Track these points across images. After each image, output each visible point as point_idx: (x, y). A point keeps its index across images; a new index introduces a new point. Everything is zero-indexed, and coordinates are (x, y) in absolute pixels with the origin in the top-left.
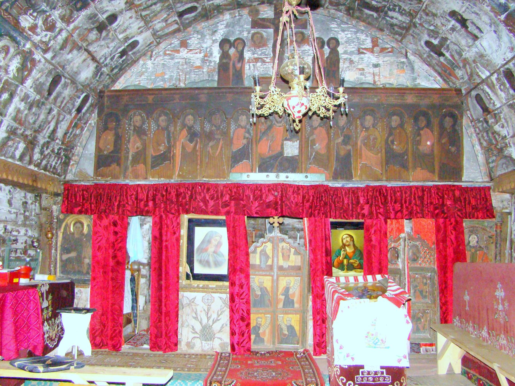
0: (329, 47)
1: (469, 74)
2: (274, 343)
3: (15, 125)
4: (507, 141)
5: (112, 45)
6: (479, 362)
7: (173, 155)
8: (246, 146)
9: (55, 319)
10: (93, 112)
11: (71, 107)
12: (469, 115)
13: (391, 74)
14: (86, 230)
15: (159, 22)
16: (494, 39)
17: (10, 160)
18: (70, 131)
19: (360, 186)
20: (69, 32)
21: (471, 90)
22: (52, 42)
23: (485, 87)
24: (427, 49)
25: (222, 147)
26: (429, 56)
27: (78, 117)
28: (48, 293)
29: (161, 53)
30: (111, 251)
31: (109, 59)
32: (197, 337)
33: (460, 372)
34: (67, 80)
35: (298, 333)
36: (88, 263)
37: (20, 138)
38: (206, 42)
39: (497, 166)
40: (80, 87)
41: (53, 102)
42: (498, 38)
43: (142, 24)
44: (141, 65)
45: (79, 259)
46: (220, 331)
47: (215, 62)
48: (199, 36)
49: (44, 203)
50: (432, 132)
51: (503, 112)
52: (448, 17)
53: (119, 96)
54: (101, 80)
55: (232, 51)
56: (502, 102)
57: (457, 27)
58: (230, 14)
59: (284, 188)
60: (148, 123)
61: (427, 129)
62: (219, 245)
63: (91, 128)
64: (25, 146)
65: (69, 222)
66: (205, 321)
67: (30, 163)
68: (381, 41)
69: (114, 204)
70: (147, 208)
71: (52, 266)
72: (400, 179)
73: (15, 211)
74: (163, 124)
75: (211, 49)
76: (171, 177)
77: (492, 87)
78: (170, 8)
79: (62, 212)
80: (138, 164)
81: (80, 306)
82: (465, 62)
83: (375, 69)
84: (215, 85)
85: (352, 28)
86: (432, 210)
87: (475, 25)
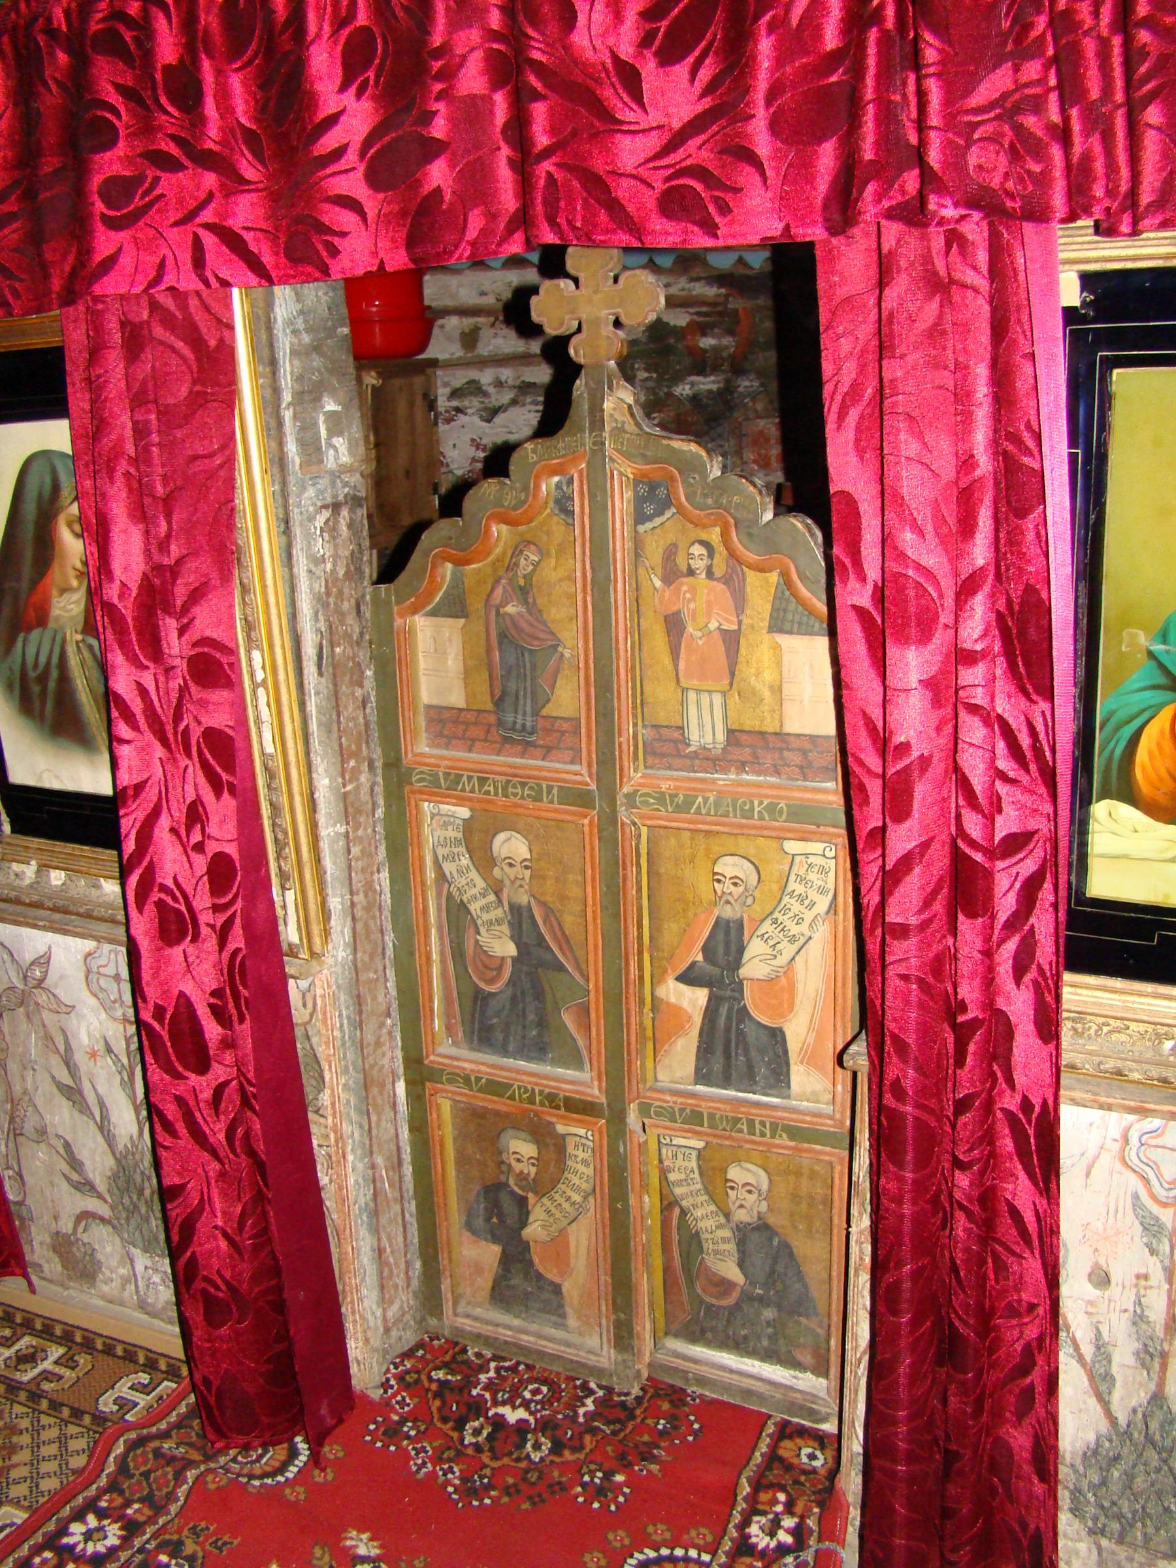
32: (102, 1219)
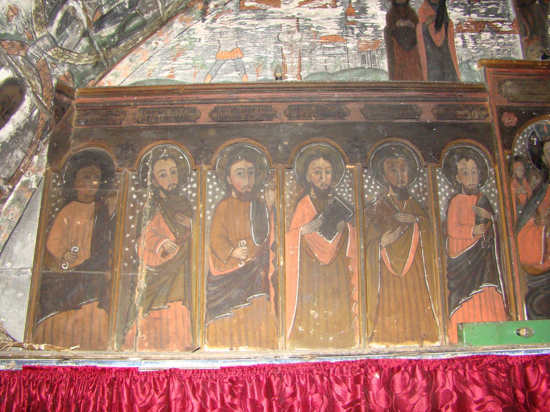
7: (276, 274)
8: (486, 244)
44: (176, 33)
47: (375, 27)
53: (115, 106)
63: (27, 196)
84: (385, 78)
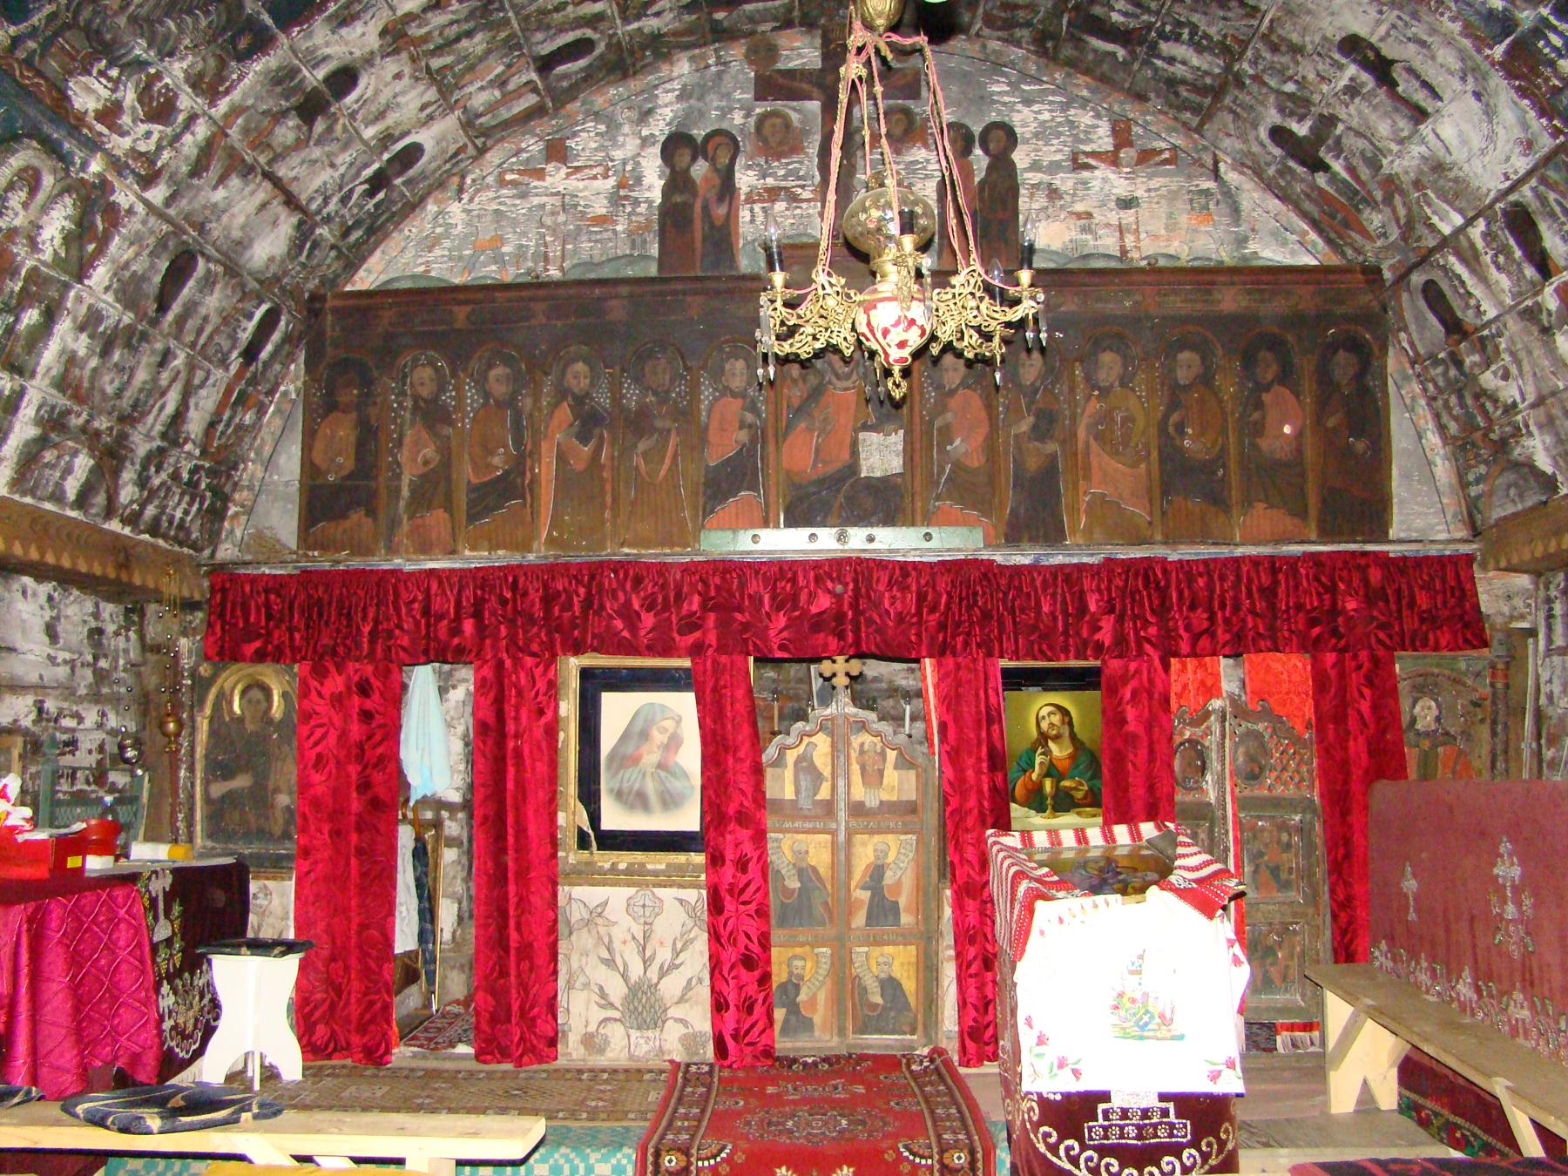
0: (986, 151)
1: (1402, 222)
2: (842, 1031)
3: (63, 401)
4: (1519, 418)
5: (345, 158)
6: (1450, 1073)
7: (532, 481)
9: (192, 974)
10: (291, 358)
11: (226, 345)
12: (1405, 345)
13: (1171, 227)
14: (277, 708)
15: (482, 88)
16: (1476, 119)
17: (48, 506)
18: (226, 417)
19: (1085, 560)
20: (215, 122)
21: (1410, 270)
22: (166, 155)
23: (1452, 259)
24: (1277, 151)
25: (675, 455)
26: (1284, 171)
27: (248, 375)
28: (169, 897)
29: (490, 179)
30: (353, 770)
31: (335, 199)
33: (1395, 1106)
34: (212, 266)
35: (912, 1000)
36: (288, 807)
37: (76, 439)
38: (623, 145)
39: (1491, 493)
40: (253, 285)
41: (174, 330)
42: (1486, 113)
43: (432, 94)
44: (430, 217)
45: (260, 796)
46: (681, 1000)
47: (650, 202)
48: (602, 128)
49: (153, 631)
50: (1297, 396)
51: (1507, 333)
52: (1337, 56)
54: (315, 262)
55: (700, 169)
56: (1501, 303)
57: (1363, 84)
58: (692, 59)
59: (861, 570)
60: (456, 388)
61: (1282, 389)
62: (674, 743)
63: (287, 407)
64: (92, 462)
65: (227, 686)
66: (636, 970)
67: (110, 511)
68: (1141, 131)
69: (359, 629)
70: (456, 641)
71: (180, 816)
72: (1205, 538)
73: (68, 656)
74: (500, 390)
75: (638, 163)
76: (526, 547)
77: (1471, 259)
78: (511, 45)
79: (207, 658)
80: (429, 508)
81: (267, 934)
82: (1391, 185)
83: (1123, 214)
84: (653, 270)
85: (1053, 93)
86: (1300, 627)
87: (1418, 77)
